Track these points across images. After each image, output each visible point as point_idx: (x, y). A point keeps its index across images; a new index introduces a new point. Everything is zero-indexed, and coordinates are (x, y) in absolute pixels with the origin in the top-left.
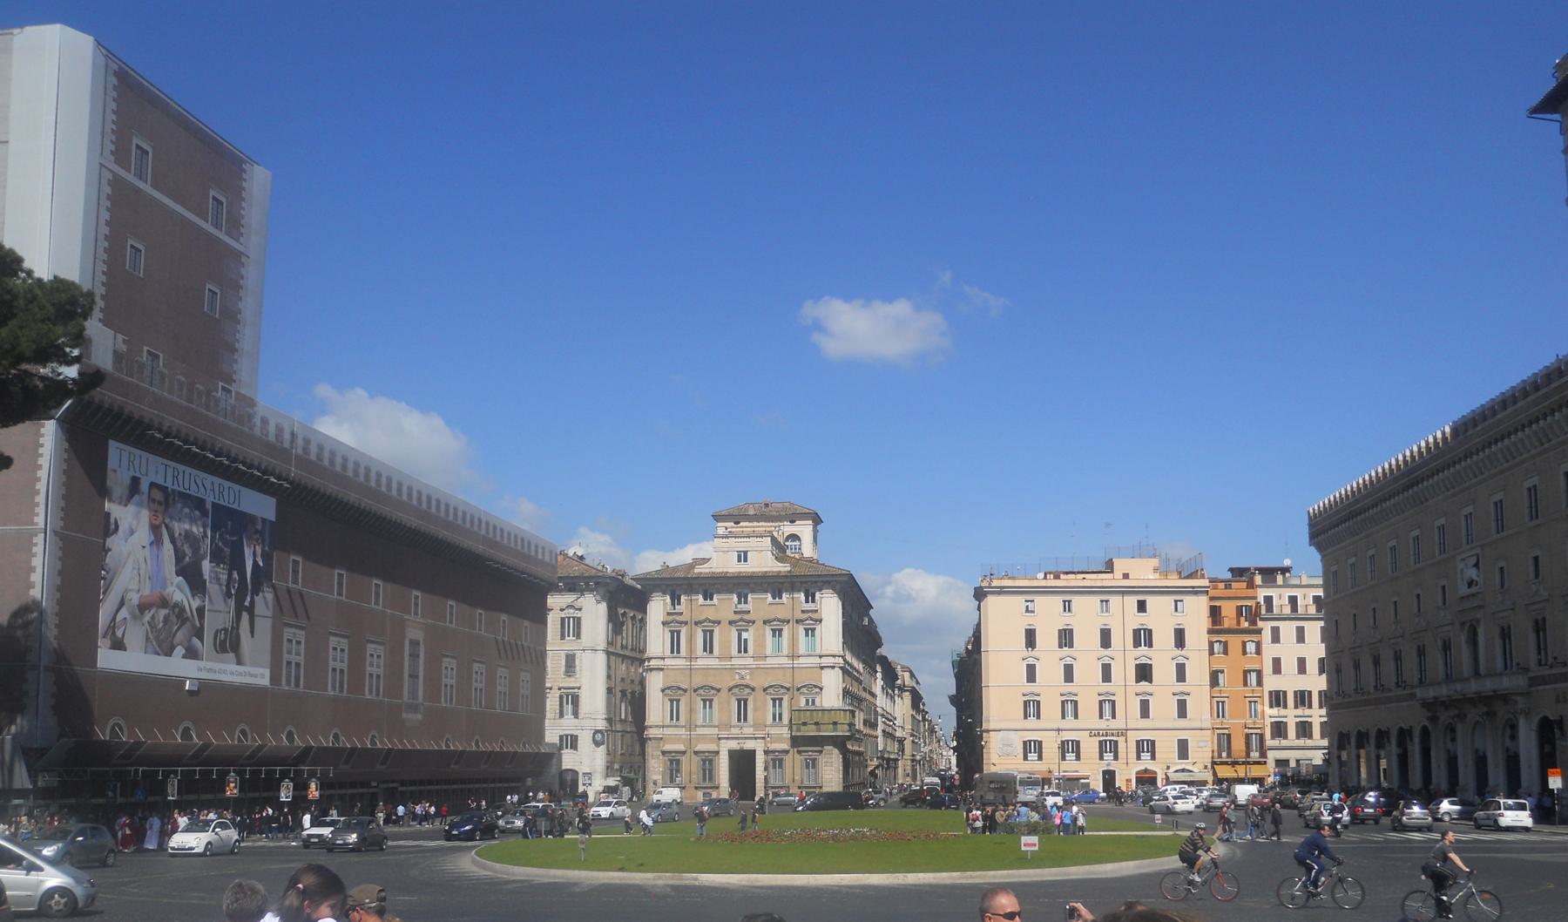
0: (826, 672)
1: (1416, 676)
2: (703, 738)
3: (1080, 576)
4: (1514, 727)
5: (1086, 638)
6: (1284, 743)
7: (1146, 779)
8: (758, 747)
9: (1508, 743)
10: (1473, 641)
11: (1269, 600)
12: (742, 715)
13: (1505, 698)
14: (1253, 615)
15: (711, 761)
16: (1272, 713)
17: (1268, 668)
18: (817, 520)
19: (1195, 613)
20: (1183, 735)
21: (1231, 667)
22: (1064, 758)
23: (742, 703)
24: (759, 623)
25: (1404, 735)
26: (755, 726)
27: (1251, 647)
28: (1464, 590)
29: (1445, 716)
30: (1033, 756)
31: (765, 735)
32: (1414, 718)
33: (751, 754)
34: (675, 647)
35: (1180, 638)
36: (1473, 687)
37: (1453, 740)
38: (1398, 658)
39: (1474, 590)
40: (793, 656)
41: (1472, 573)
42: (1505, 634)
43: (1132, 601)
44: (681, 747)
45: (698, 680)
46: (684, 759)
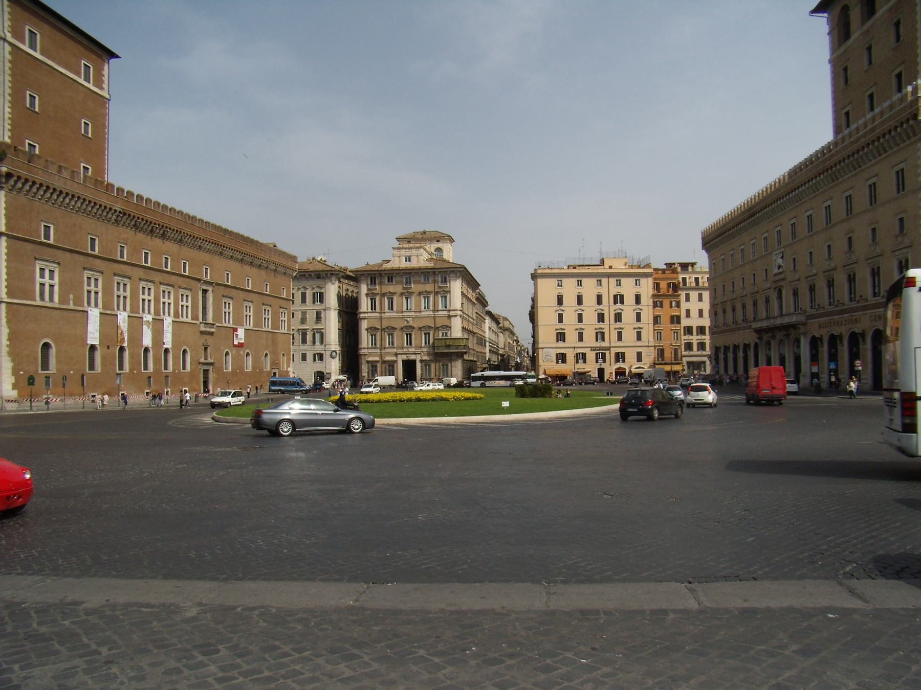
1: (752, 316)
4: (798, 341)
5: (589, 300)
6: (691, 353)
7: (620, 372)
8: (418, 358)
9: (796, 349)
10: (780, 297)
11: (684, 279)
12: (410, 342)
13: (794, 326)
14: (676, 288)
15: (393, 366)
16: (685, 338)
17: (683, 314)
19: (646, 288)
20: (639, 350)
21: (666, 313)
22: (577, 362)
23: (409, 336)
25: (746, 347)
26: (416, 347)
27: (674, 304)
28: (776, 271)
29: (766, 337)
32: (750, 337)
33: (414, 362)
34: (373, 307)
35: (638, 299)
36: (779, 321)
37: (770, 349)
38: (744, 307)
39: (781, 270)
40: (435, 310)
41: (780, 261)
42: (795, 293)
43: (613, 281)
44: (377, 359)
45: (385, 324)
46: (379, 365)
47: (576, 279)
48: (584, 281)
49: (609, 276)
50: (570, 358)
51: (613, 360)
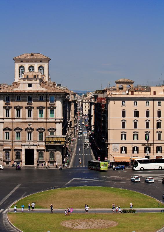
0: (58, 124)
2: (17, 145)
3: (140, 92)
8: (35, 148)
12: (30, 138)
15: (19, 153)
18: (48, 60)
22: (133, 153)
23: (30, 134)
24: (35, 108)
30: (124, 152)
31: (37, 144)
33: (33, 150)
43: (156, 103)
44: (9, 148)
45: (15, 126)
46: (11, 152)
47: (133, 102)
48: (139, 102)
49: (154, 99)
50: (129, 148)
51: (155, 151)
